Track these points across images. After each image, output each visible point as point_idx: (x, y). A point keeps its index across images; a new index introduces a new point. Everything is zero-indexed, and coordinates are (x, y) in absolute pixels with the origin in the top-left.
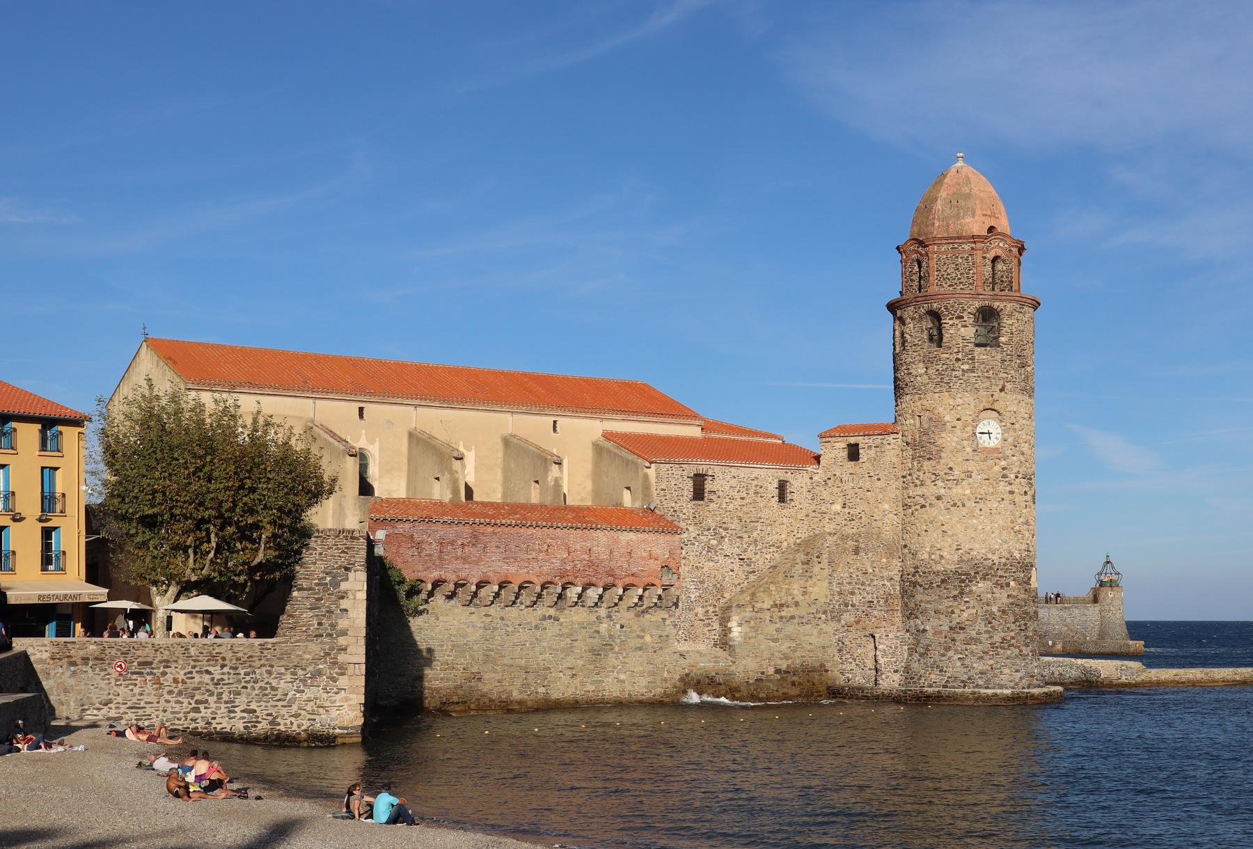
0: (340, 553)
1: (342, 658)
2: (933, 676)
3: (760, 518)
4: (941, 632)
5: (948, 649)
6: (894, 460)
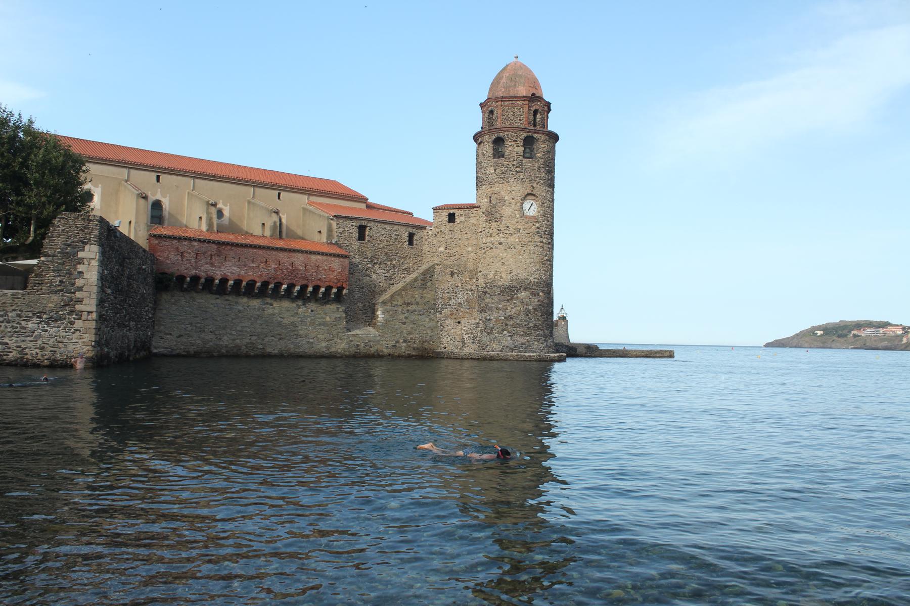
0: (79, 231)
1: (78, 307)
2: (494, 345)
3: (397, 253)
4: (500, 320)
5: (503, 331)
6: (475, 222)
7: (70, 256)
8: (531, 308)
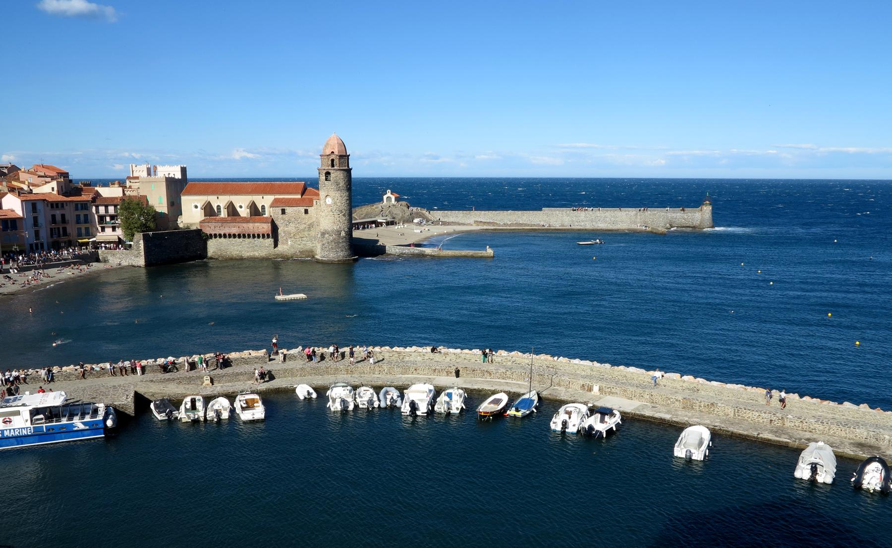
7: (138, 242)
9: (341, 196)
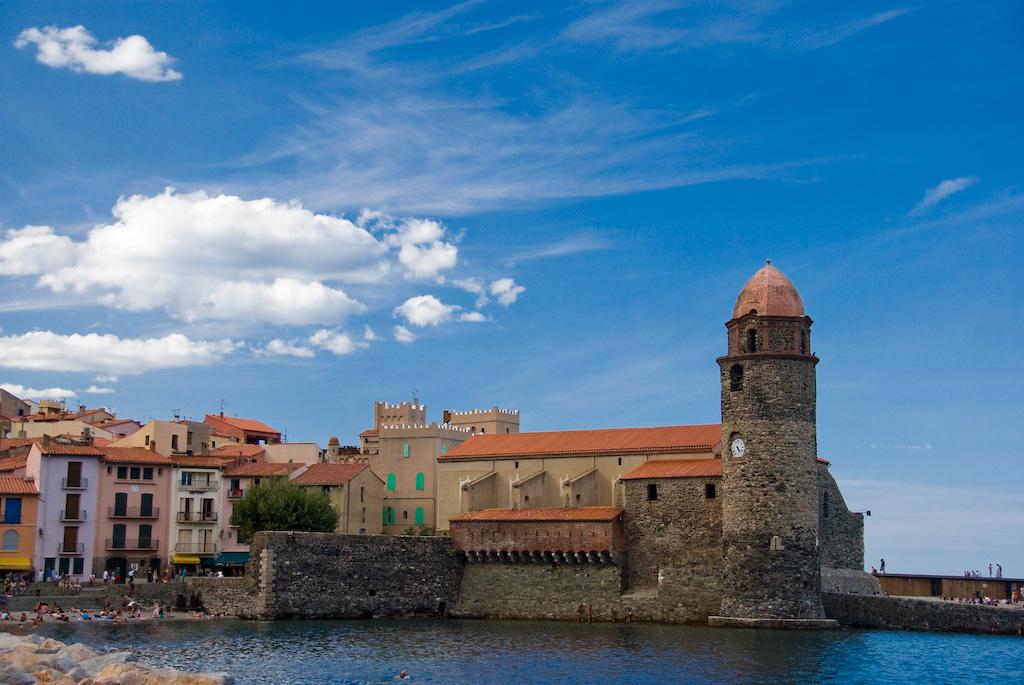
8: (737, 564)
9: (772, 433)
